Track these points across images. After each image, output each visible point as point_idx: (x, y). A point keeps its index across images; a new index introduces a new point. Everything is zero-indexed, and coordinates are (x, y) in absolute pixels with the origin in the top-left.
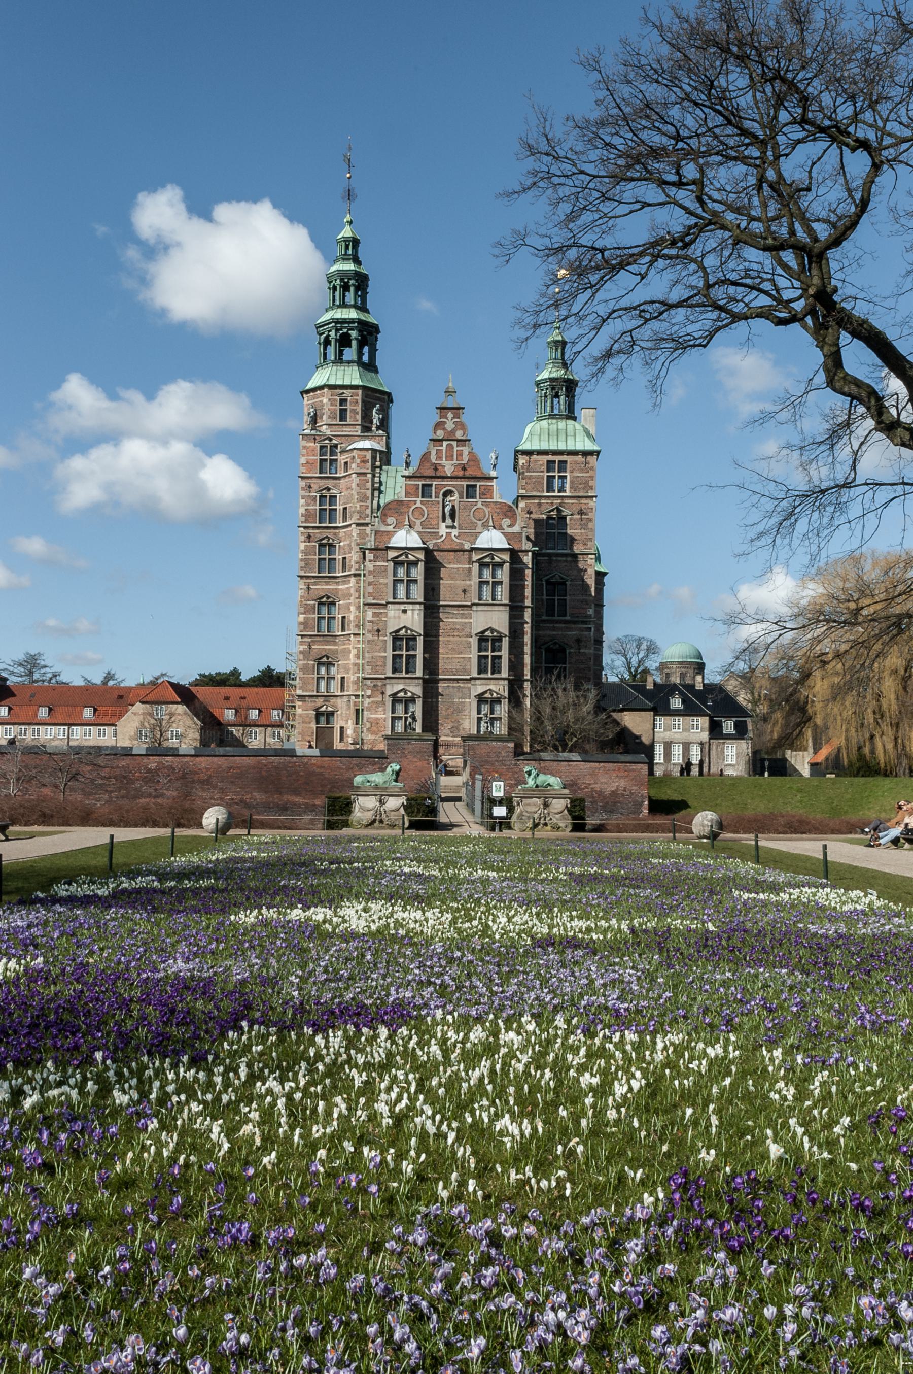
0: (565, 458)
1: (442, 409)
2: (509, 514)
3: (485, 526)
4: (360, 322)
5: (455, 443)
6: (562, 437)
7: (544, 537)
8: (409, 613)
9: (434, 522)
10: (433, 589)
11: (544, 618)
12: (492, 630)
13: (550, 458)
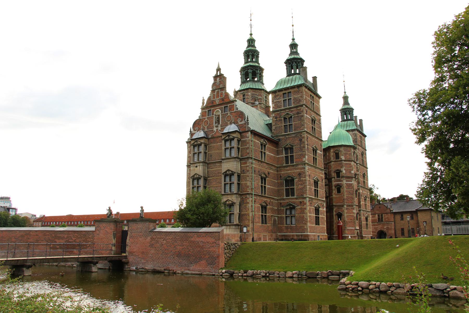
1: (215, 77)
3: (231, 124)
4: (250, 66)
5: (219, 90)
7: (283, 127)
8: (198, 167)
10: (211, 156)
11: (285, 165)
12: (229, 170)
13: (284, 92)
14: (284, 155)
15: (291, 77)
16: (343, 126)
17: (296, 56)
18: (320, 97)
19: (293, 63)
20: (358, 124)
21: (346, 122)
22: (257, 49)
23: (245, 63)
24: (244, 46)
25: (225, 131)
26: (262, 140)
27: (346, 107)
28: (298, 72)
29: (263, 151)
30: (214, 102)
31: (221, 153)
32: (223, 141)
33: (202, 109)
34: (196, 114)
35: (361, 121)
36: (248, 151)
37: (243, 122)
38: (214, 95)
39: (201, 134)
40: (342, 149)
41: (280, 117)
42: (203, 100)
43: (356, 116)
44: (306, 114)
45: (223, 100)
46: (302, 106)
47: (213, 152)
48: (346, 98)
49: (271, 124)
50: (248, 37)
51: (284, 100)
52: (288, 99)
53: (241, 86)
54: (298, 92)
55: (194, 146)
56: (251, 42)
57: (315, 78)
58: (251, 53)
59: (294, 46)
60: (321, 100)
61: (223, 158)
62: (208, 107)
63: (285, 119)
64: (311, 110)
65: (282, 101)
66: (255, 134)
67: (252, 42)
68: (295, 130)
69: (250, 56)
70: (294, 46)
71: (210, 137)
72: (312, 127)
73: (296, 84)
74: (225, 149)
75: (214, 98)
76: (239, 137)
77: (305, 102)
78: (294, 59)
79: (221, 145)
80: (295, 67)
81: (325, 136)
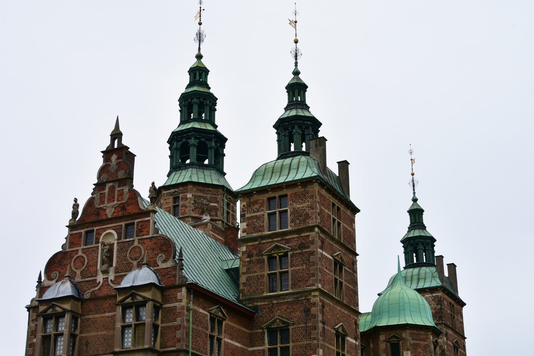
0: (284, 192)
1: (107, 154)
2: (164, 248)
3: (140, 266)
4: (194, 129)
5: (116, 185)
6: (286, 172)
7: (266, 279)
9: (92, 269)
10: (87, 344)
13: (271, 194)
14: (267, 346)
15: (288, 161)
16: (409, 279)
17: (301, 113)
18: (355, 210)
19: (293, 128)
20: (446, 274)
21: (416, 270)
22: (211, 91)
23: (182, 122)
24: (181, 83)
25: (126, 283)
26: (214, 309)
27: (417, 233)
28: (304, 149)
29: (216, 334)
30: (101, 212)
31: (113, 336)
32: (119, 309)
33: (71, 227)
34: (56, 240)
35: (452, 267)
36: (178, 334)
37: (169, 264)
38: (102, 196)
39: (65, 289)
40: (406, 334)
41: (260, 254)
42: (76, 206)
43: (441, 257)
44: (322, 248)
45: (123, 207)
46: (311, 229)
47: (93, 334)
48: (416, 214)
49: (237, 270)
50: (192, 62)
51: (269, 214)
52: (280, 212)
53: (169, 175)
54: (302, 197)
55: (46, 318)
56: (198, 74)
57: (344, 165)
58: (198, 100)
59: (297, 89)
60: (357, 215)
61: (117, 350)
62: (85, 223)
63: (271, 258)
64: (333, 239)
65: (266, 216)
66: (197, 292)
67: (200, 75)
68: (294, 285)
69: (195, 108)
70: (297, 89)
71: (87, 296)
72: (336, 280)
73: (299, 177)
74: (124, 328)
75: (103, 202)
76: (159, 298)
77: (319, 221)
78: (297, 118)
79: (113, 317)
80: (297, 137)
81: (366, 303)
